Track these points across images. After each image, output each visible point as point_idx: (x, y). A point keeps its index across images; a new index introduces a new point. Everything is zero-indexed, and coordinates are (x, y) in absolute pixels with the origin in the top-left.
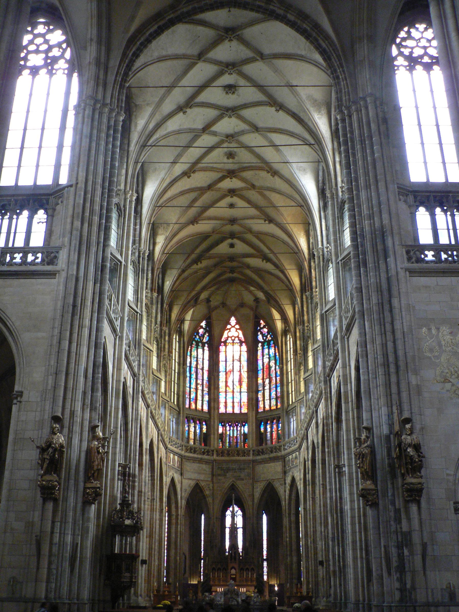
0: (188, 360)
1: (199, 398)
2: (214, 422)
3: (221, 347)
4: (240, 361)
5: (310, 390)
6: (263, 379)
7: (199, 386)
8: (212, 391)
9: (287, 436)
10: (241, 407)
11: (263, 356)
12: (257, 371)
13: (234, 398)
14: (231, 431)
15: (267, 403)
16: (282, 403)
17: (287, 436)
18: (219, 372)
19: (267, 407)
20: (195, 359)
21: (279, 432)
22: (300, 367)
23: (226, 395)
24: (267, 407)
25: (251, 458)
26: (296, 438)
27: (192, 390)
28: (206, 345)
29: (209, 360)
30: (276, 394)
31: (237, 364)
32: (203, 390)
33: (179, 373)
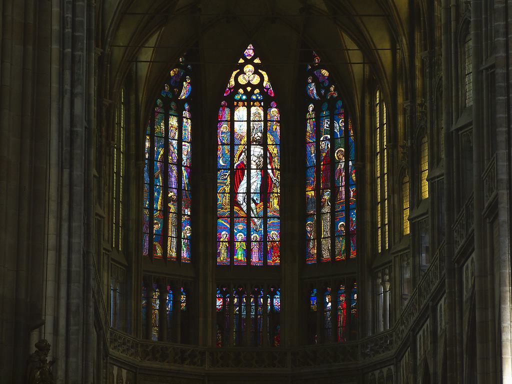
0: (147, 144)
1: (172, 232)
4: (263, 143)
5: (424, 246)
6: (317, 190)
7: (170, 205)
9: (370, 325)
11: (318, 133)
12: (305, 168)
13: (248, 231)
15: (326, 244)
16: (360, 248)
17: (370, 325)
18: (216, 168)
19: (326, 255)
20: (163, 141)
21: (353, 311)
22: (402, 175)
23: (232, 225)
24: (326, 255)
26: (391, 336)
27: (156, 214)
28: (187, 107)
30: (347, 227)
31: (257, 151)
32: (179, 214)
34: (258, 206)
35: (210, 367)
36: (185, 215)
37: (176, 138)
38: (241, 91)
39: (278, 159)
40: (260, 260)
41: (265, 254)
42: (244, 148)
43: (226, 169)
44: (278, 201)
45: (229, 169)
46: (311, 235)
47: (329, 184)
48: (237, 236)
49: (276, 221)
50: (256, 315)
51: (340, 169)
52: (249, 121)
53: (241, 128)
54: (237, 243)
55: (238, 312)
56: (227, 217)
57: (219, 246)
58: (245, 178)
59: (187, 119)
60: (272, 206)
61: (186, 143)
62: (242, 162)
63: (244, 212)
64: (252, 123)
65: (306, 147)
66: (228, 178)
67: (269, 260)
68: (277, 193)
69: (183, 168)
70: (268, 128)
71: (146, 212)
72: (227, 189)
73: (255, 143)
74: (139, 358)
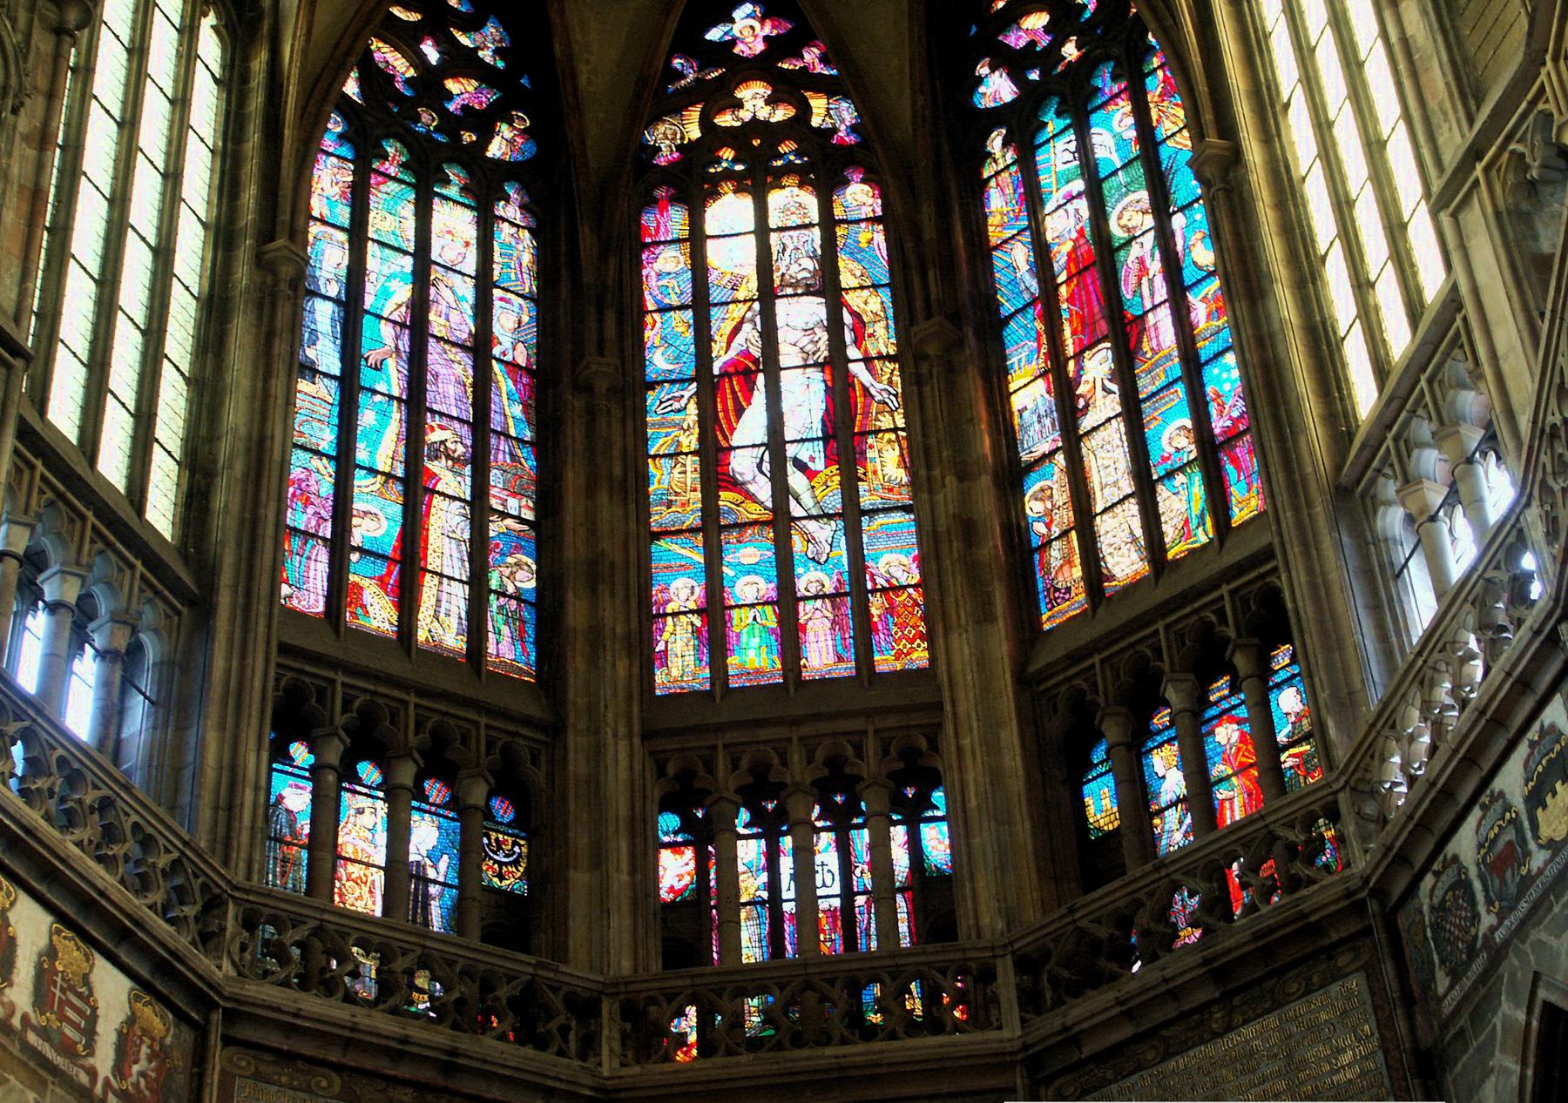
2: (597, 753)
3: (649, 219)
4: (827, 285)
7: (436, 467)
8: (573, 507)
10: (864, 633)
11: (1032, 197)
12: (993, 326)
14: (786, 865)
18: (633, 384)
19: (1125, 564)
20: (408, 262)
24: (1125, 564)
25: (1010, 1031)
29: (545, 300)
31: (800, 317)
32: (479, 508)
33: (215, 308)
34: (820, 478)
35: (623, 1065)
36: (504, 515)
37: (470, 266)
38: (727, 154)
39: (887, 327)
40: (840, 659)
41: (864, 633)
42: (750, 309)
43: (682, 381)
44: (902, 455)
45: (691, 380)
46: (1048, 525)
47: (1103, 327)
48: (737, 590)
49: (897, 517)
50: (848, 894)
51: (1141, 261)
52: (762, 231)
53: (732, 258)
54: (735, 613)
55: (765, 895)
56: (692, 530)
57: (662, 631)
58: (759, 397)
59: (518, 226)
60: (875, 472)
61: (509, 295)
62: (746, 354)
63: (761, 503)
64: (774, 238)
65: (990, 258)
66: (692, 409)
67: (881, 652)
68: (895, 430)
69: (496, 366)
70: (840, 242)
71: (327, 469)
72: (690, 441)
73: (789, 291)
74: (226, 964)
